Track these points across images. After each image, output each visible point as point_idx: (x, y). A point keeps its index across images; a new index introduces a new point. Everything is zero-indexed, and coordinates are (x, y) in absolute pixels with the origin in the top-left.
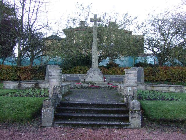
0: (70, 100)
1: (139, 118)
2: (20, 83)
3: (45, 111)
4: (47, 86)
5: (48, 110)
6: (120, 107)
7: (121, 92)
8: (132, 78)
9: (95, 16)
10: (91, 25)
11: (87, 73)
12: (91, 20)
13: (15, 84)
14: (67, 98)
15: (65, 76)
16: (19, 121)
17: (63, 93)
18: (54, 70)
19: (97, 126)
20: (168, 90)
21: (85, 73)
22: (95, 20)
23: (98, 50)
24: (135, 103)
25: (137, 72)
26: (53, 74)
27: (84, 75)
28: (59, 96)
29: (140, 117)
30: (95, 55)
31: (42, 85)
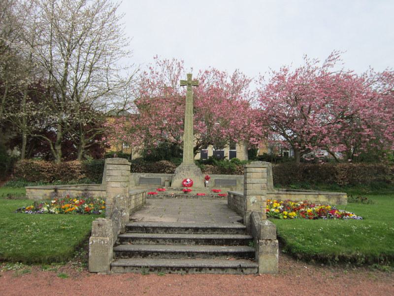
0: (145, 220)
1: (274, 253)
2: (56, 190)
3: (96, 243)
4: (104, 194)
5: (102, 240)
6: (237, 233)
7: (236, 205)
8: (257, 180)
9: (190, 76)
10: (181, 90)
11: (176, 172)
12: (183, 84)
13: (46, 190)
14: (138, 216)
15: (137, 176)
16: (63, 259)
17: (133, 206)
18: (116, 166)
19: (195, 269)
20: (315, 200)
21: (172, 172)
22: (190, 83)
23: (194, 134)
24: (267, 225)
25: (266, 169)
26: (114, 173)
27: (171, 175)
28: (125, 214)
29: (276, 253)
30: (189, 142)
31: (96, 193)
